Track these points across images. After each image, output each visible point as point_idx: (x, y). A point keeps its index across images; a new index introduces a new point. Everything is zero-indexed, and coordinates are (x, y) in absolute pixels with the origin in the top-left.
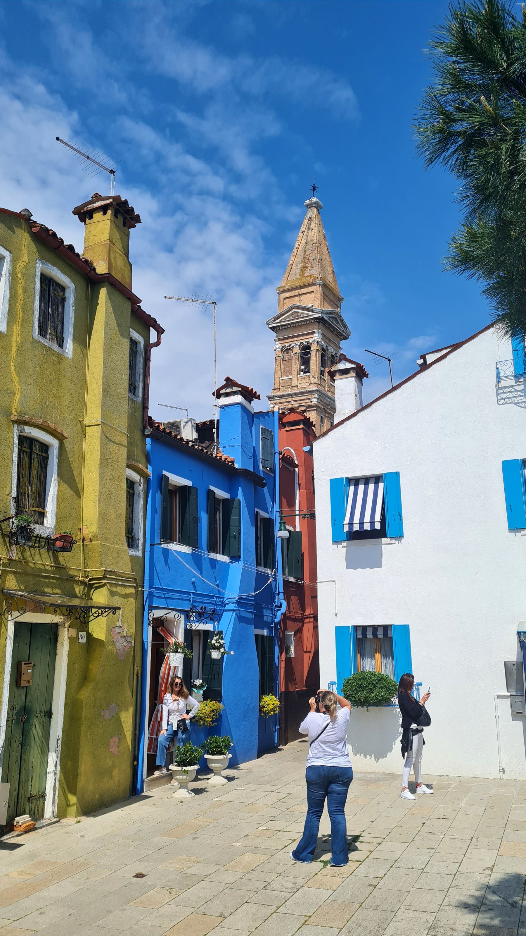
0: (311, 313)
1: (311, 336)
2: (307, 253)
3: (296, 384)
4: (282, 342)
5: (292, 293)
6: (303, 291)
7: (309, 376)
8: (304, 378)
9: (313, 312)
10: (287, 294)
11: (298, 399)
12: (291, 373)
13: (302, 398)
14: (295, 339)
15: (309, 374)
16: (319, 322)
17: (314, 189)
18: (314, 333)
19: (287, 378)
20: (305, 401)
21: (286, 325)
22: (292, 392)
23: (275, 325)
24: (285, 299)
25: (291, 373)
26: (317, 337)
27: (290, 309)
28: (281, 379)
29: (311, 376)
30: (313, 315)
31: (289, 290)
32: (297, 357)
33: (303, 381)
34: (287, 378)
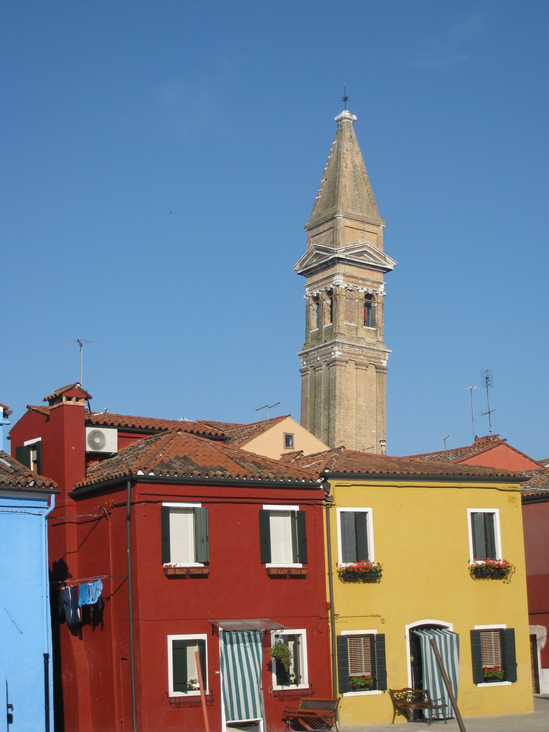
0: (384, 262)
4: (346, 278)
7: (376, 332)
9: (385, 260)
14: (361, 282)
17: (345, 99)
18: (381, 283)
23: (344, 257)
29: (378, 334)
34: (351, 325)
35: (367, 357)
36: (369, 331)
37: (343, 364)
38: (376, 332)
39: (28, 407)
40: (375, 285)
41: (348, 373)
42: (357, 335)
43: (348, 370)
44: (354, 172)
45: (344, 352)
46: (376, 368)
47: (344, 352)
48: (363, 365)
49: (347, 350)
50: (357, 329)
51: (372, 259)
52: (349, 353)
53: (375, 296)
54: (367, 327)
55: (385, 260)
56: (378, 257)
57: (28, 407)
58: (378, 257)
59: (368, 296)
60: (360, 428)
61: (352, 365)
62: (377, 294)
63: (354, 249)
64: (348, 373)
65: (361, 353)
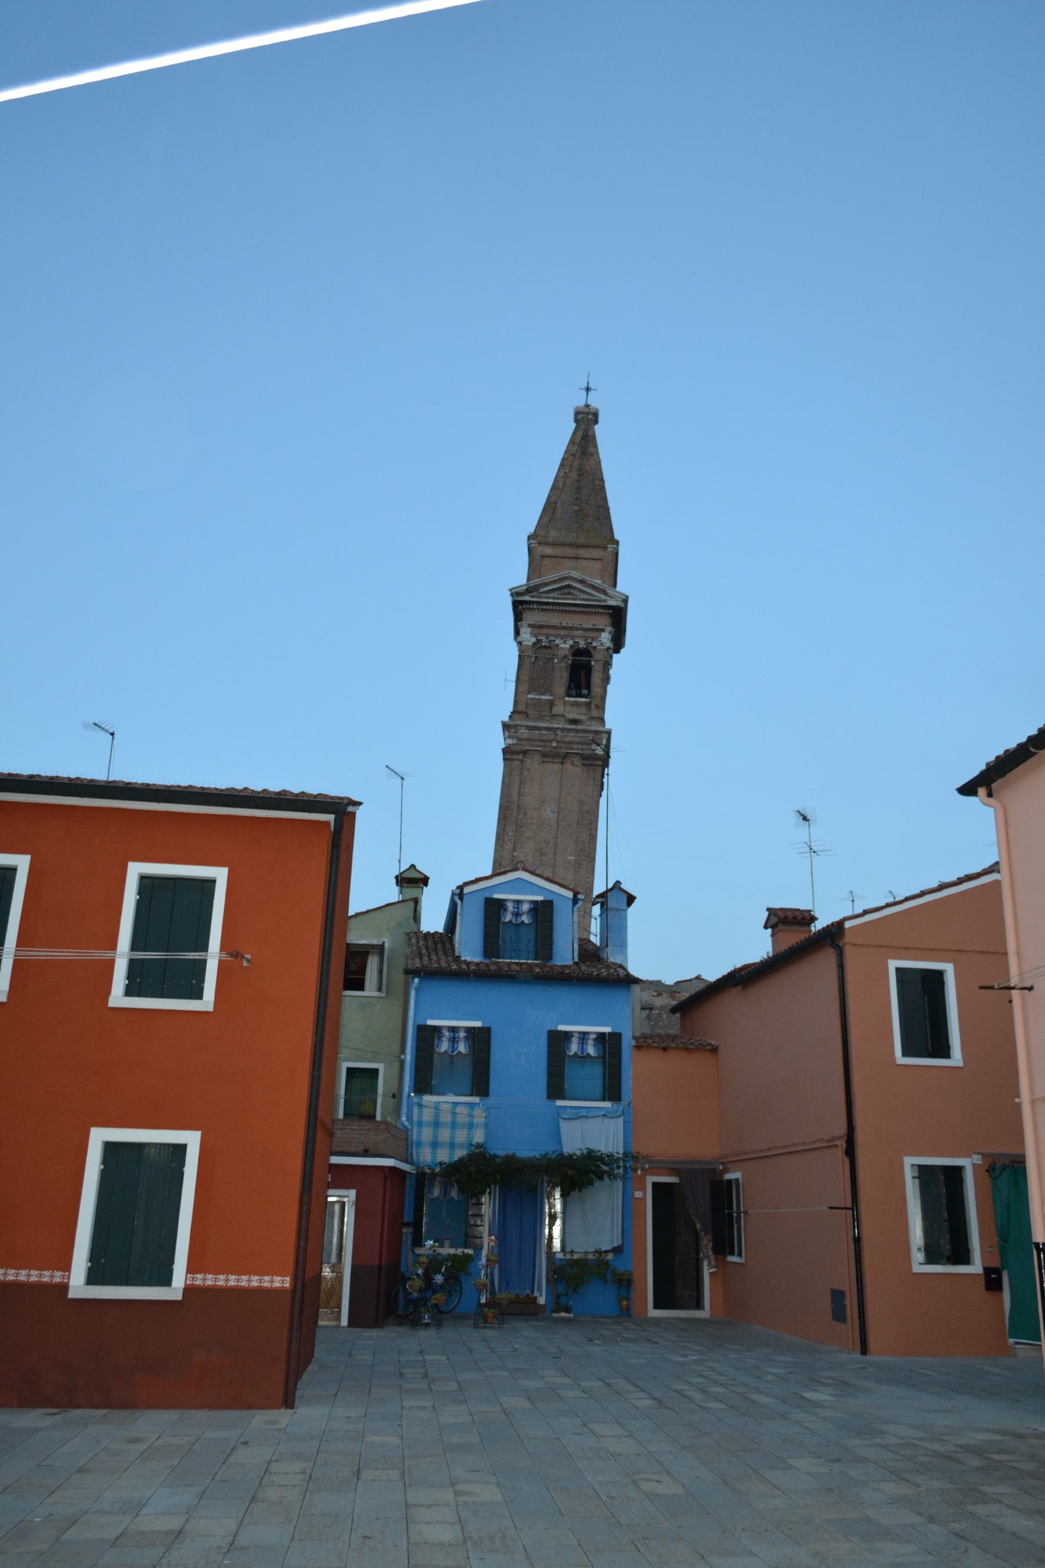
0: (604, 597)
1: (594, 634)
2: (585, 492)
3: (561, 712)
4: (536, 631)
5: (558, 551)
6: (582, 553)
9: (606, 594)
10: (548, 551)
11: (567, 739)
13: (578, 740)
14: (563, 632)
15: (588, 700)
16: (611, 615)
18: (603, 630)
19: (543, 697)
20: (580, 746)
22: (556, 726)
24: (543, 557)
25: (548, 690)
27: (560, 580)
28: (530, 696)
29: (593, 706)
30: (605, 601)
31: (553, 545)
32: (563, 664)
33: (575, 709)
35: (564, 742)
37: (515, 757)
39: (768, 909)
40: (590, 634)
41: (528, 770)
42: (551, 711)
44: (579, 481)
45: (519, 739)
46: (584, 757)
47: (519, 739)
48: (557, 755)
49: (526, 736)
50: (551, 704)
51: (585, 597)
52: (528, 740)
53: (592, 651)
54: (571, 699)
55: (606, 594)
56: (592, 592)
57: (768, 909)
58: (592, 592)
59: (577, 652)
60: (542, 854)
61: (537, 758)
62: (595, 647)
63: (546, 584)
64: (528, 770)
65: (552, 737)
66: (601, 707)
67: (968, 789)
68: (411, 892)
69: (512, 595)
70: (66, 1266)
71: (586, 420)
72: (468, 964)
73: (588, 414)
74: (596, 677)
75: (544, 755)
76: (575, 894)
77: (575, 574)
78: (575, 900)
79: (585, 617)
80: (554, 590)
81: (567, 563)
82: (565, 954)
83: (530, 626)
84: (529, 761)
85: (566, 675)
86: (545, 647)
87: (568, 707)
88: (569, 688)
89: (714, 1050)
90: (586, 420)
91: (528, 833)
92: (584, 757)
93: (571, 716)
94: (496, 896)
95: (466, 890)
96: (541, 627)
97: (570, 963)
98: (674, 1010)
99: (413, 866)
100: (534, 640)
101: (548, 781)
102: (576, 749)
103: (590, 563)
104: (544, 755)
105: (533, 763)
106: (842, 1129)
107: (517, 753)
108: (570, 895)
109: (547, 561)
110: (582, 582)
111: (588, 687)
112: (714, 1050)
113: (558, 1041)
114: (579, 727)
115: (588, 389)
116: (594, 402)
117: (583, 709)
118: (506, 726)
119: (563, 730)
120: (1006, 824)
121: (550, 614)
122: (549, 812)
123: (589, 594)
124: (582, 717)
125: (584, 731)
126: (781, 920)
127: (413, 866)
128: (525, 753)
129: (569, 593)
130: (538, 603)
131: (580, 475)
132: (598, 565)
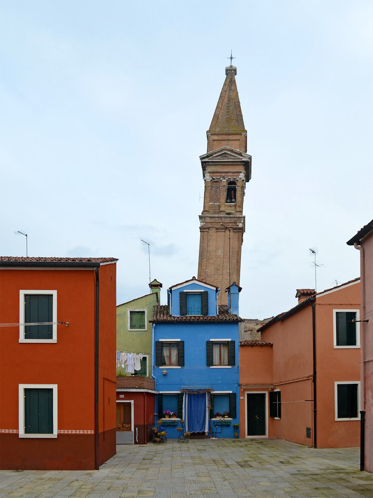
0: (241, 157)
2: (231, 108)
4: (212, 175)
5: (220, 137)
6: (231, 137)
8: (231, 206)
9: (242, 156)
10: (216, 137)
12: (218, 200)
14: (223, 174)
16: (244, 165)
18: (241, 172)
21: (216, 162)
25: (218, 200)
26: (242, 176)
27: (222, 151)
31: (217, 135)
32: (224, 189)
33: (229, 208)
36: (231, 206)
38: (235, 206)
40: (235, 174)
43: (211, 234)
44: (228, 103)
45: (206, 223)
47: (206, 223)
49: (209, 221)
50: (219, 206)
52: (210, 223)
61: (214, 230)
63: (215, 153)
65: (220, 221)
66: (241, 207)
67: (350, 243)
68: (156, 290)
69: (201, 159)
70: (17, 428)
71: (231, 72)
72: (174, 317)
73: (231, 70)
74: (238, 194)
75: (217, 229)
76: (217, 288)
77: (228, 147)
78: (217, 291)
79: (233, 167)
80: (219, 155)
81: (224, 142)
82: (213, 312)
83: (209, 172)
84: (211, 232)
85: (225, 193)
86: (216, 182)
87: (226, 207)
88: (227, 199)
89: (271, 346)
90: (231, 72)
91: (212, 262)
92: (234, 229)
93: (228, 211)
94: (185, 291)
95: (173, 289)
96: (214, 172)
97: (215, 315)
98: (258, 331)
99: (155, 280)
100: (211, 179)
101: (220, 240)
102: (230, 225)
103: (234, 142)
104: (217, 229)
105: (212, 232)
106: (312, 373)
107: (206, 228)
108: (215, 289)
109: (215, 142)
110: (232, 151)
111: (235, 198)
112: (271, 346)
113: (210, 345)
114: (231, 216)
115: (231, 58)
116: (234, 65)
117: (233, 208)
118: (200, 217)
119: (225, 217)
120: (364, 256)
121: (218, 167)
122: (220, 253)
123: (234, 156)
124: (233, 212)
125: (234, 217)
126: (301, 294)
127: (155, 280)
128: (209, 228)
129: (225, 157)
130: (212, 162)
131: (229, 101)
132: (238, 142)
